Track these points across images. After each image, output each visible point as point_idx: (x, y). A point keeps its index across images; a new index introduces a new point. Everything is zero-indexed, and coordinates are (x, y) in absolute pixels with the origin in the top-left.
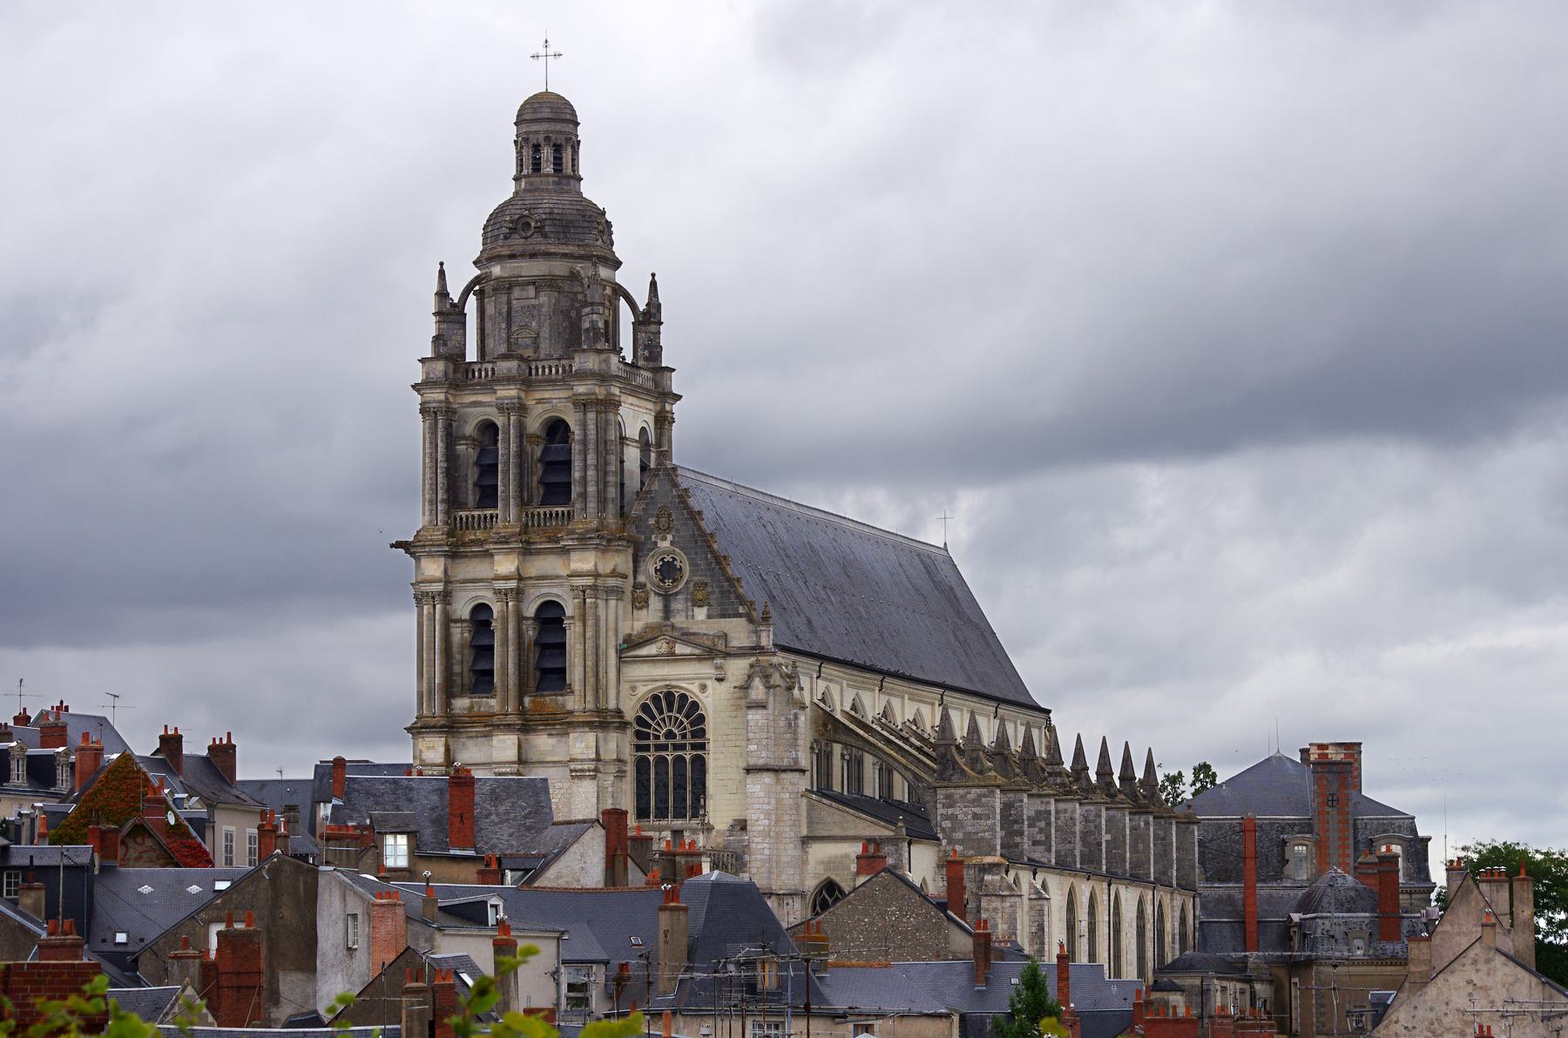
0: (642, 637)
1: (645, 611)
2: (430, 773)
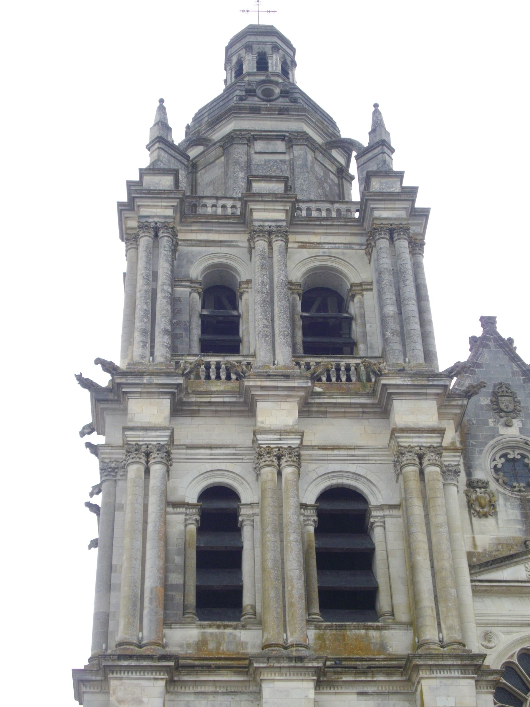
1: (490, 521)
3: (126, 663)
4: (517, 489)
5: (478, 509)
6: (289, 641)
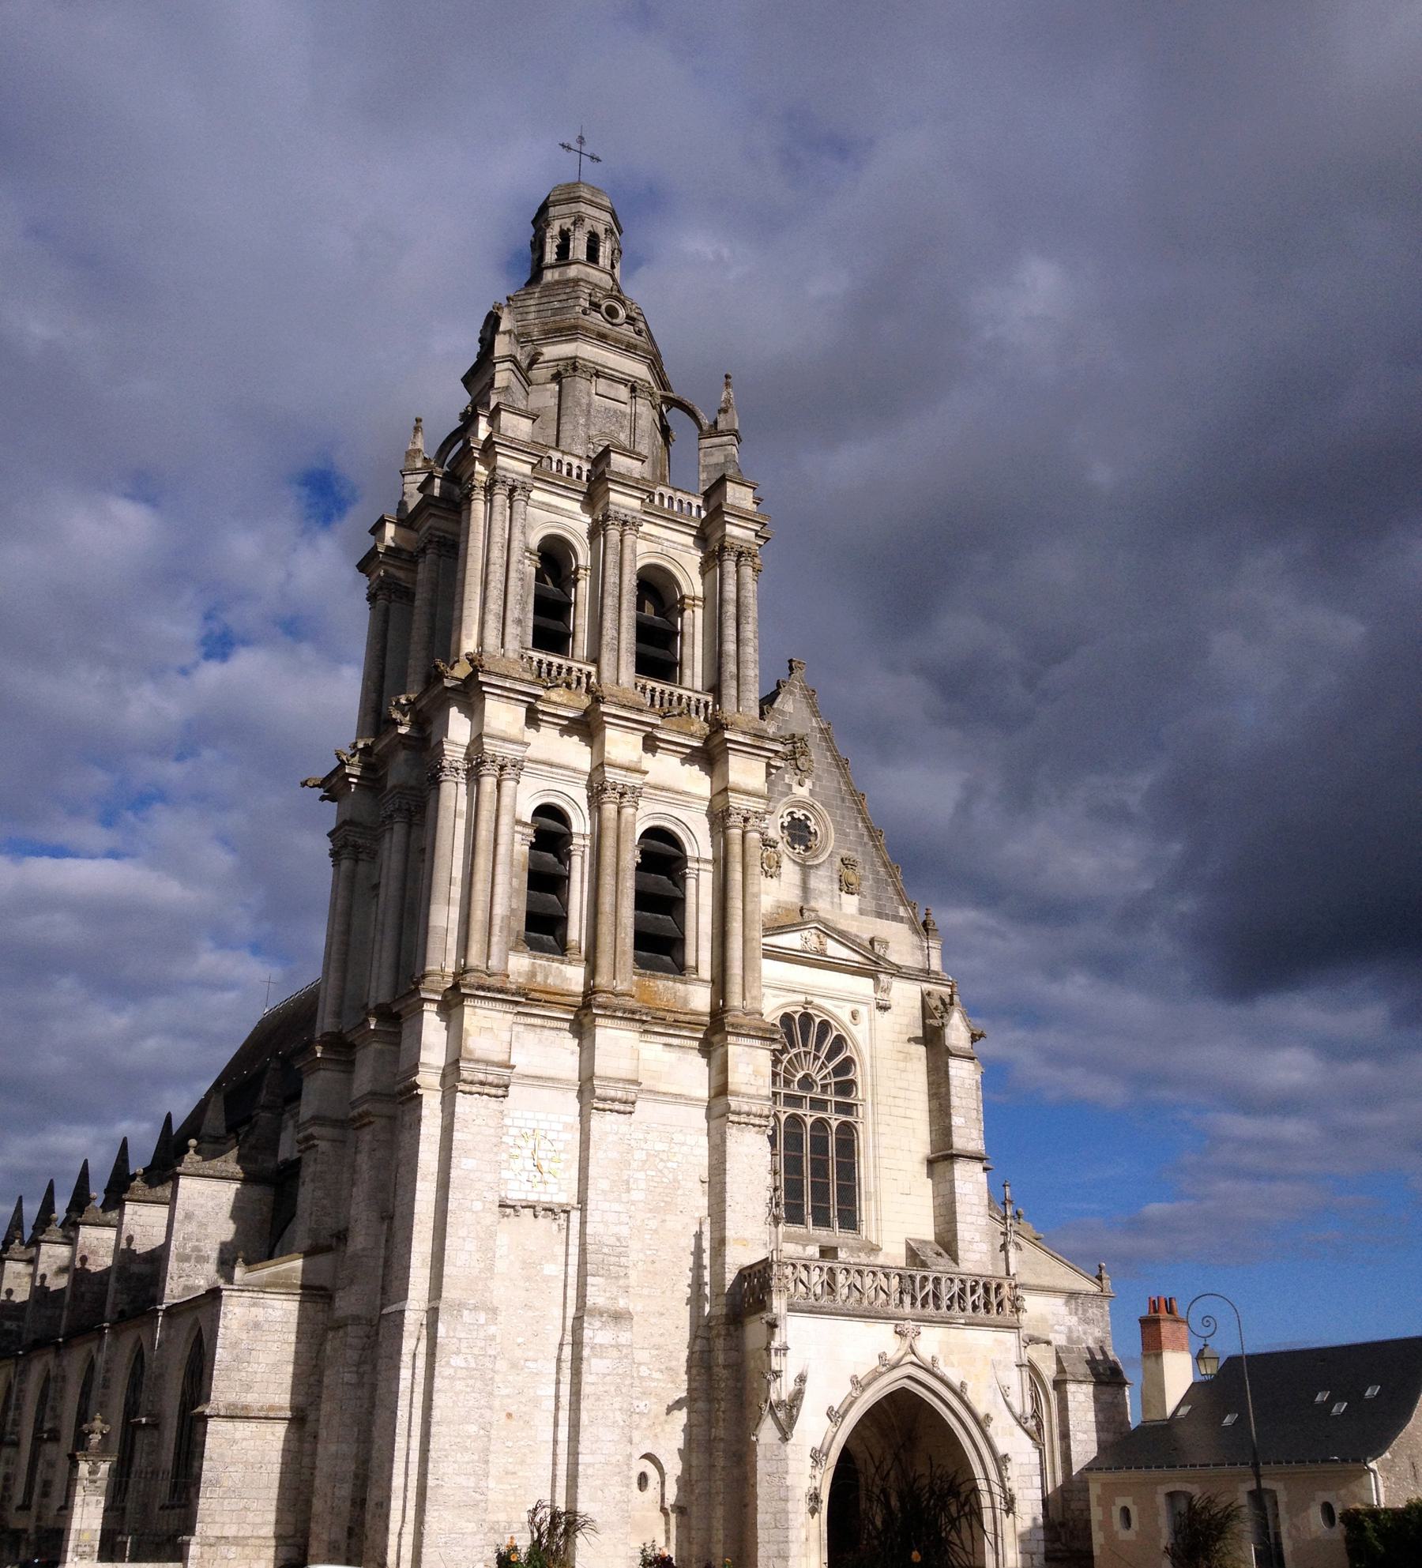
0: (776, 920)
2: (481, 1077)
3: (482, 994)
4: (797, 851)
5: (766, 868)
6: (617, 989)
